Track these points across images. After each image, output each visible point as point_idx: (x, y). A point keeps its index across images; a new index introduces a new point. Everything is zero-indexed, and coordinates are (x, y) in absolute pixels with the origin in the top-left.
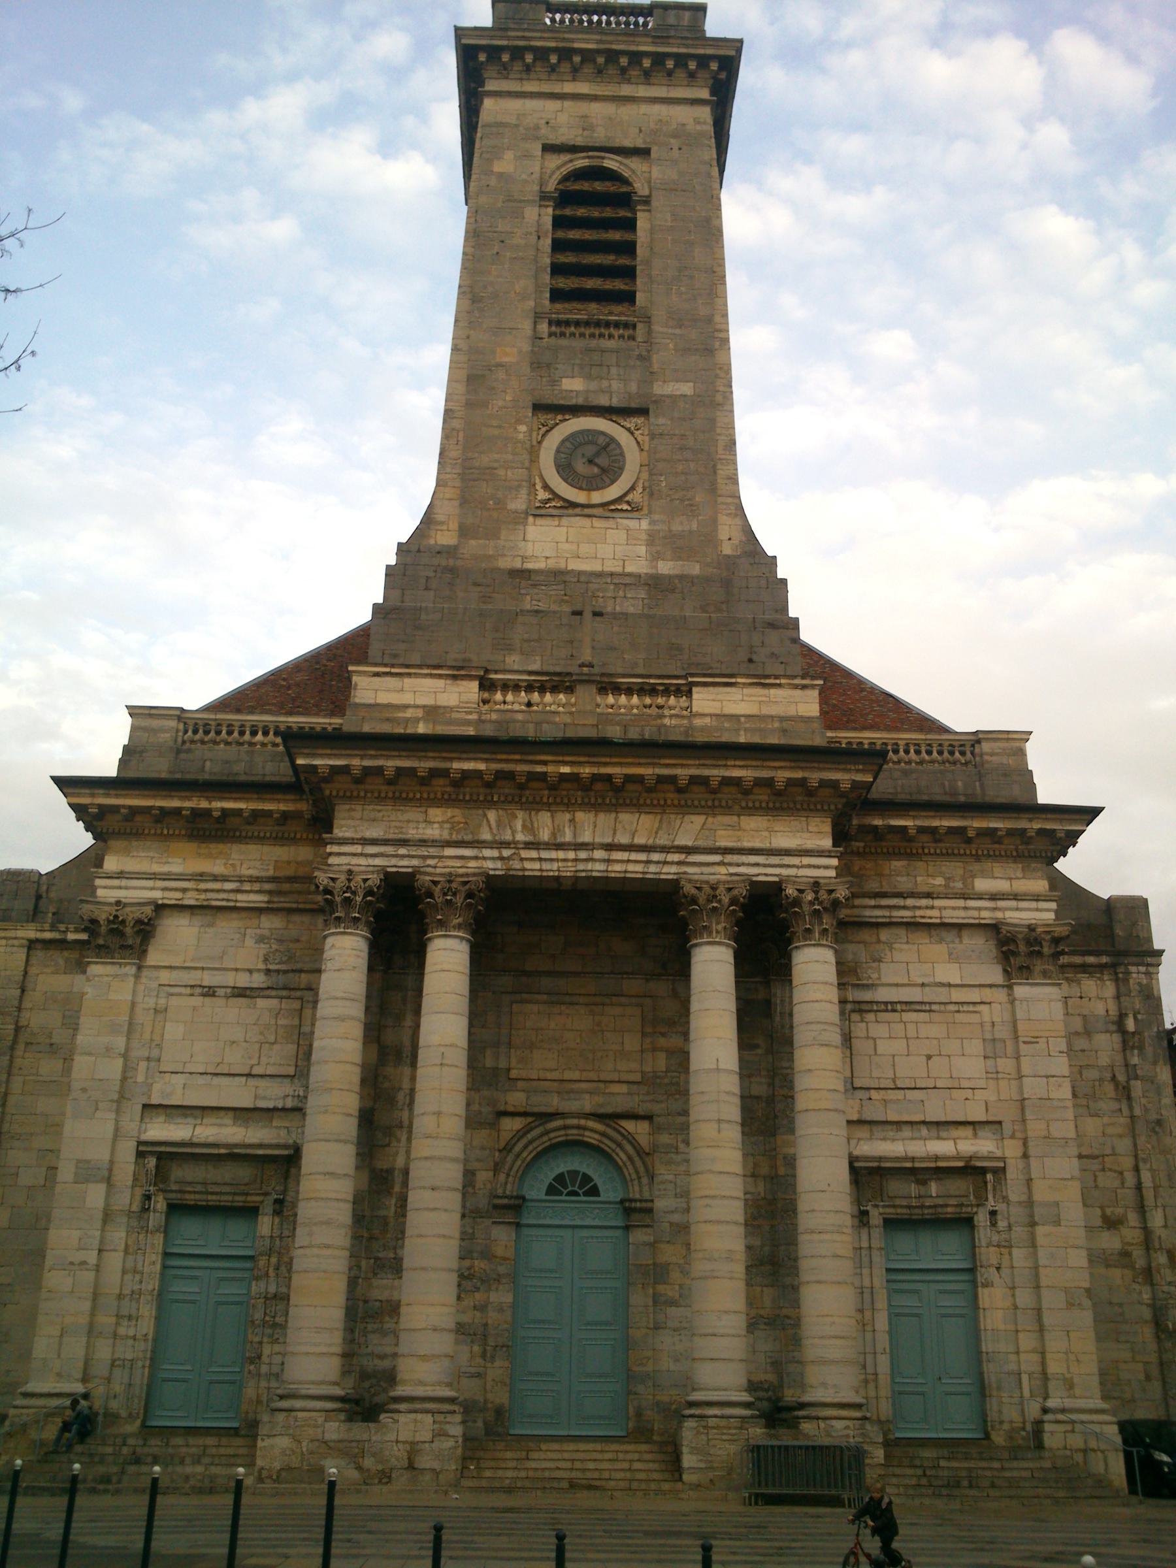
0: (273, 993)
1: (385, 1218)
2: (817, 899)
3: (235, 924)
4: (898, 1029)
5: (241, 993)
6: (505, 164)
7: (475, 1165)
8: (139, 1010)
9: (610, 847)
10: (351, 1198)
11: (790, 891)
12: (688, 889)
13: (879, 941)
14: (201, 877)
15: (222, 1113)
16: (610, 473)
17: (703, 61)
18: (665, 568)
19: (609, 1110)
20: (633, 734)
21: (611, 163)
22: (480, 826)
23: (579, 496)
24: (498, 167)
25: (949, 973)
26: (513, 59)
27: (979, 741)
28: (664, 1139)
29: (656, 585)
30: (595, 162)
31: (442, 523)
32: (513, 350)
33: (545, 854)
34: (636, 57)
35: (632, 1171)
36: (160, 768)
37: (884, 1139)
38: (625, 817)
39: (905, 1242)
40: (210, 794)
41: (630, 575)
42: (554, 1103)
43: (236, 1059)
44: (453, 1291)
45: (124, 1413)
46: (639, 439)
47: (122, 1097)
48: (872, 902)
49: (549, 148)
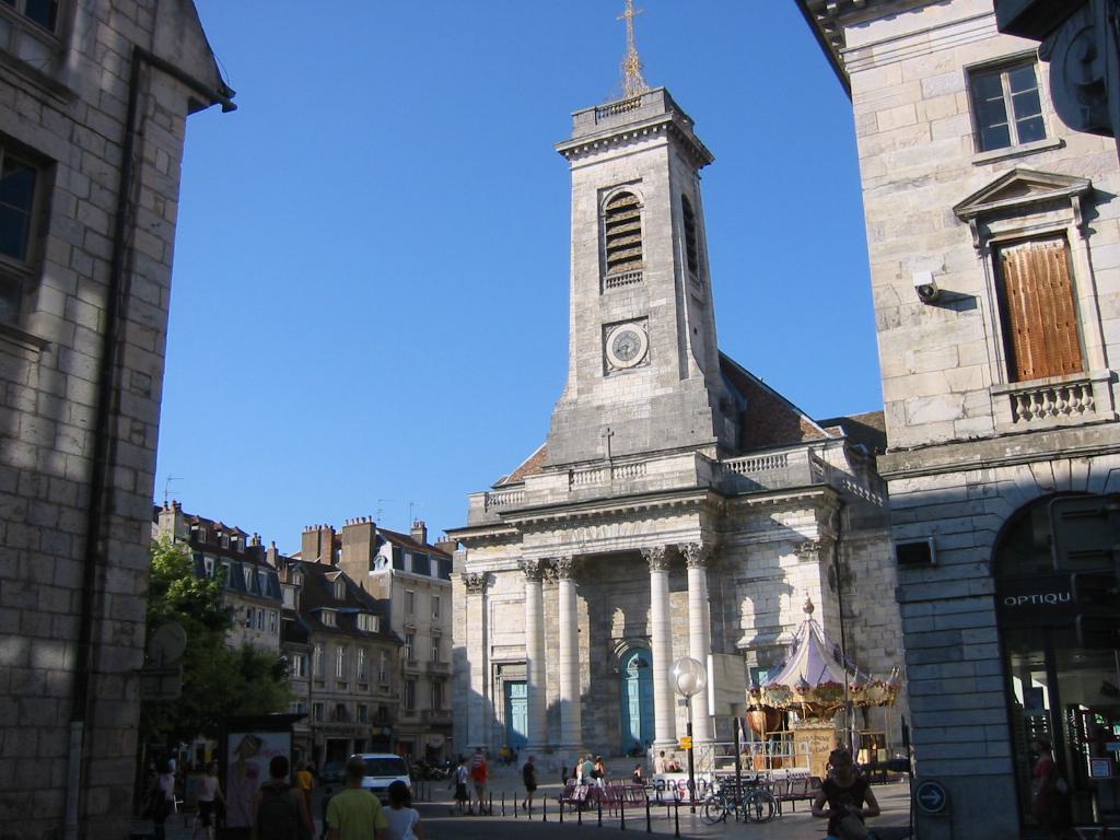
5: (517, 602)
9: (617, 538)
12: (643, 554)
13: (746, 552)
14: (498, 559)
17: (659, 126)
18: (659, 392)
21: (628, 189)
23: (624, 365)
29: (654, 401)
30: (621, 191)
33: (594, 544)
34: (630, 134)
49: (600, 191)
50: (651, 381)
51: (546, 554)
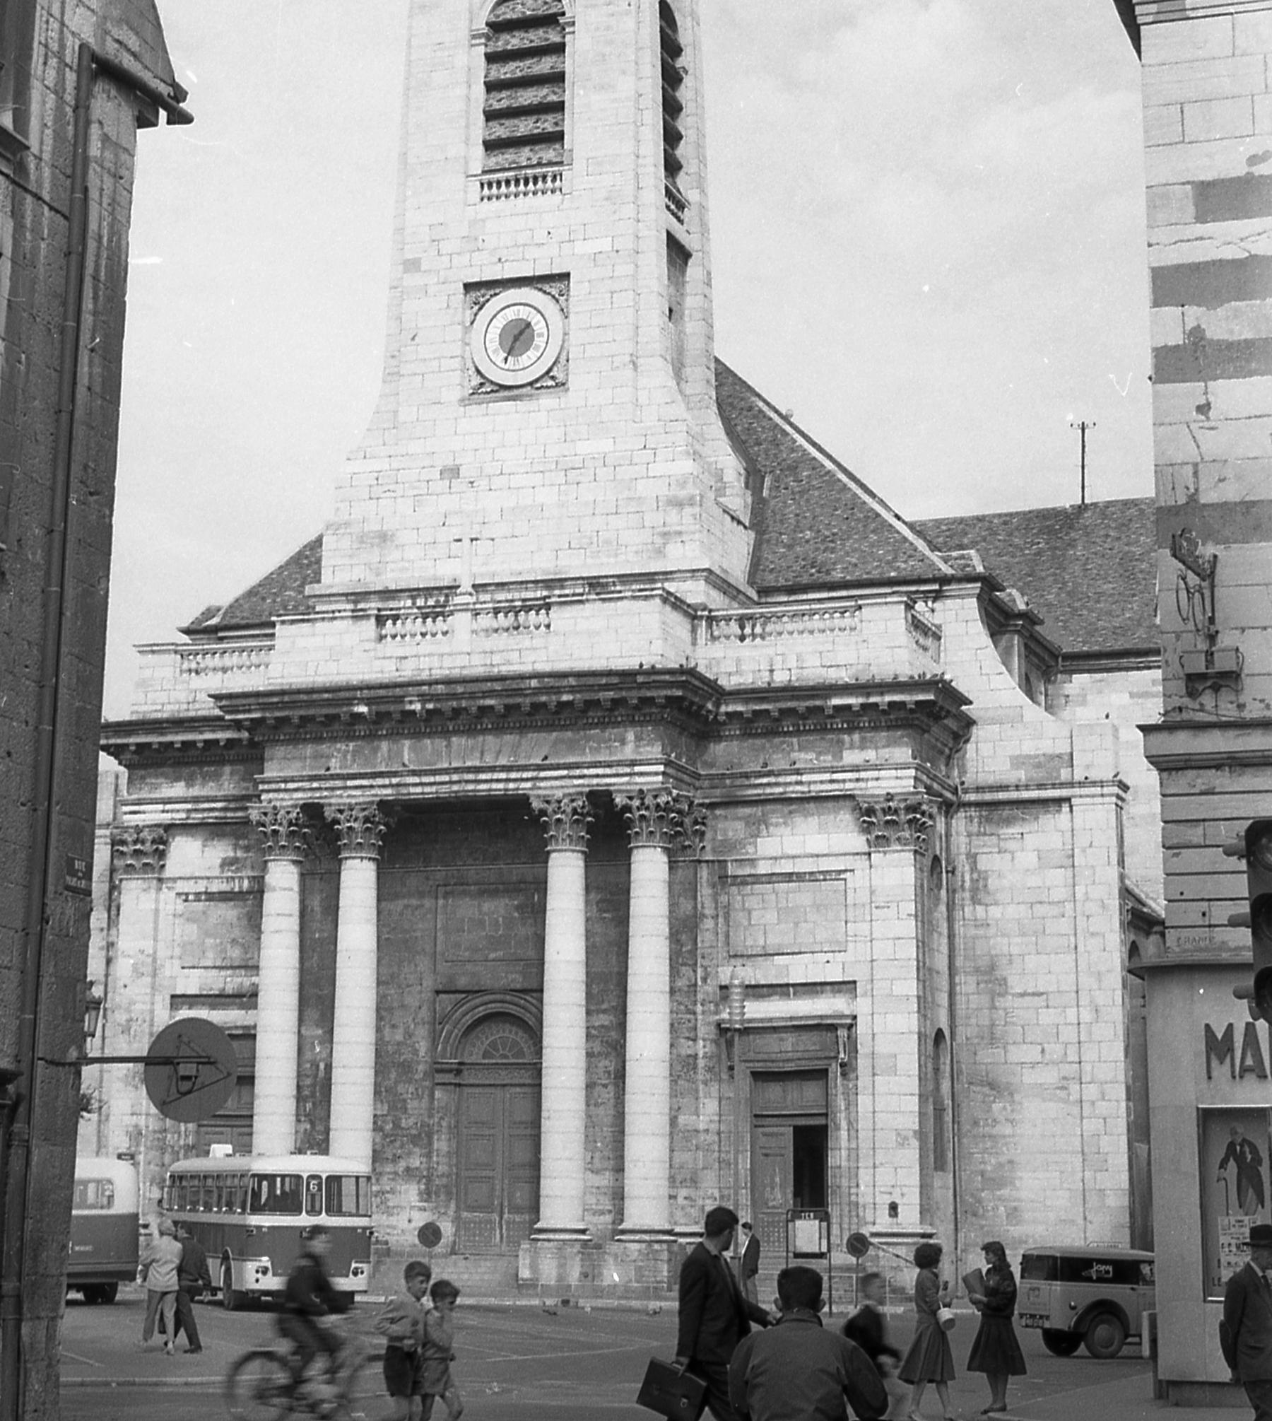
2: (643, 804)
11: (619, 800)
12: (536, 804)
25: (817, 843)
27: (860, 607)
39: (774, 1091)
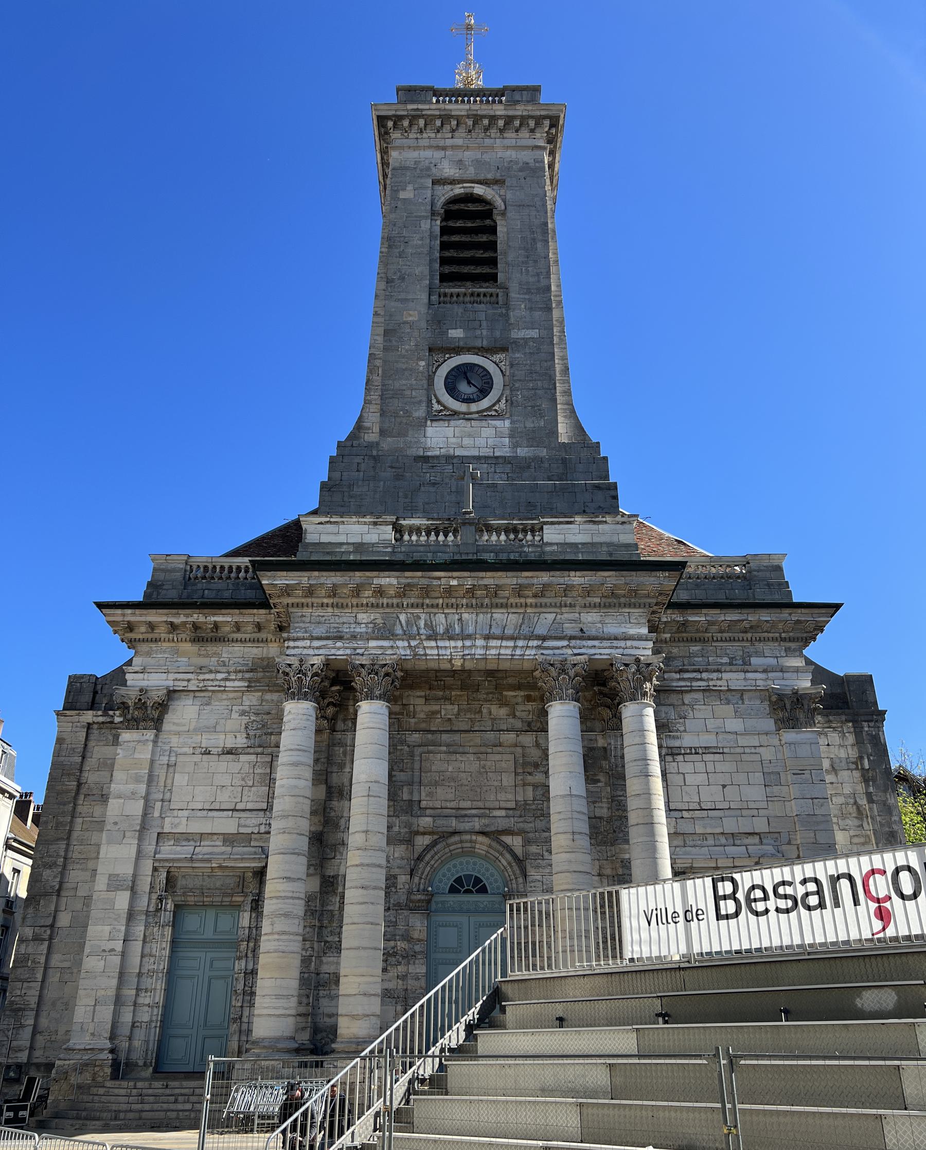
0: (252, 750)
1: (332, 911)
2: (638, 670)
3: (225, 703)
4: (700, 766)
6: (407, 194)
7: (396, 871)
8: (156, 765)
10: (303, 896)
13: (684, 704)
15: (215, 837)
16: (484, 392)
17: (539, 120)
18: (522, 452)
19: (493, 829)
20: (503, 556)
21: (479, 190)
22: (395, 625)
24: (402, 195)
26: (411, 125)
28: (533, 849)
30: (468, 190)
31: (369, 429)
32: (416, 312)
33: (440, 643)
34: (493, 119)
35: (511, 873)
36: (171, 595)
37: (695, 846)
38: (499, 615)
40: (206, 611)
41: (497, 458)
42: (453, 823)
43: (225, 798)
44: (380, 965)
45: (141, 1063)
46: (503, 368)
47: (144, 828)
48: (678, 676)
50: (511, 436)
51: (340, 651)
